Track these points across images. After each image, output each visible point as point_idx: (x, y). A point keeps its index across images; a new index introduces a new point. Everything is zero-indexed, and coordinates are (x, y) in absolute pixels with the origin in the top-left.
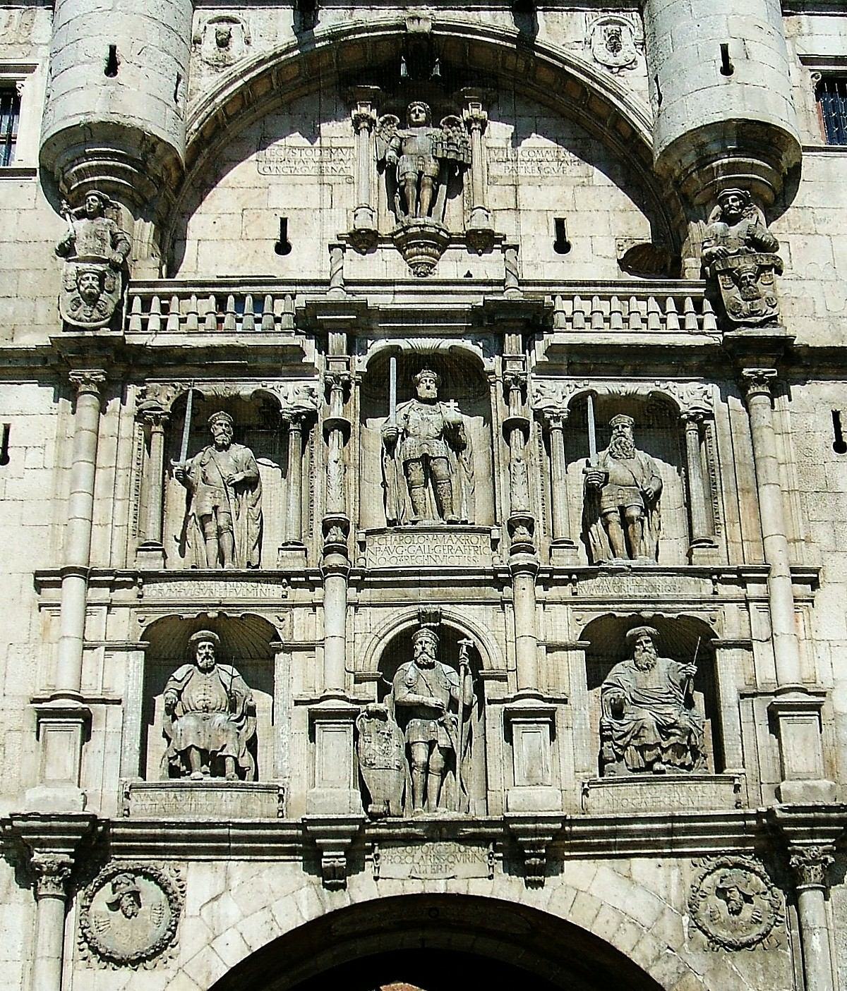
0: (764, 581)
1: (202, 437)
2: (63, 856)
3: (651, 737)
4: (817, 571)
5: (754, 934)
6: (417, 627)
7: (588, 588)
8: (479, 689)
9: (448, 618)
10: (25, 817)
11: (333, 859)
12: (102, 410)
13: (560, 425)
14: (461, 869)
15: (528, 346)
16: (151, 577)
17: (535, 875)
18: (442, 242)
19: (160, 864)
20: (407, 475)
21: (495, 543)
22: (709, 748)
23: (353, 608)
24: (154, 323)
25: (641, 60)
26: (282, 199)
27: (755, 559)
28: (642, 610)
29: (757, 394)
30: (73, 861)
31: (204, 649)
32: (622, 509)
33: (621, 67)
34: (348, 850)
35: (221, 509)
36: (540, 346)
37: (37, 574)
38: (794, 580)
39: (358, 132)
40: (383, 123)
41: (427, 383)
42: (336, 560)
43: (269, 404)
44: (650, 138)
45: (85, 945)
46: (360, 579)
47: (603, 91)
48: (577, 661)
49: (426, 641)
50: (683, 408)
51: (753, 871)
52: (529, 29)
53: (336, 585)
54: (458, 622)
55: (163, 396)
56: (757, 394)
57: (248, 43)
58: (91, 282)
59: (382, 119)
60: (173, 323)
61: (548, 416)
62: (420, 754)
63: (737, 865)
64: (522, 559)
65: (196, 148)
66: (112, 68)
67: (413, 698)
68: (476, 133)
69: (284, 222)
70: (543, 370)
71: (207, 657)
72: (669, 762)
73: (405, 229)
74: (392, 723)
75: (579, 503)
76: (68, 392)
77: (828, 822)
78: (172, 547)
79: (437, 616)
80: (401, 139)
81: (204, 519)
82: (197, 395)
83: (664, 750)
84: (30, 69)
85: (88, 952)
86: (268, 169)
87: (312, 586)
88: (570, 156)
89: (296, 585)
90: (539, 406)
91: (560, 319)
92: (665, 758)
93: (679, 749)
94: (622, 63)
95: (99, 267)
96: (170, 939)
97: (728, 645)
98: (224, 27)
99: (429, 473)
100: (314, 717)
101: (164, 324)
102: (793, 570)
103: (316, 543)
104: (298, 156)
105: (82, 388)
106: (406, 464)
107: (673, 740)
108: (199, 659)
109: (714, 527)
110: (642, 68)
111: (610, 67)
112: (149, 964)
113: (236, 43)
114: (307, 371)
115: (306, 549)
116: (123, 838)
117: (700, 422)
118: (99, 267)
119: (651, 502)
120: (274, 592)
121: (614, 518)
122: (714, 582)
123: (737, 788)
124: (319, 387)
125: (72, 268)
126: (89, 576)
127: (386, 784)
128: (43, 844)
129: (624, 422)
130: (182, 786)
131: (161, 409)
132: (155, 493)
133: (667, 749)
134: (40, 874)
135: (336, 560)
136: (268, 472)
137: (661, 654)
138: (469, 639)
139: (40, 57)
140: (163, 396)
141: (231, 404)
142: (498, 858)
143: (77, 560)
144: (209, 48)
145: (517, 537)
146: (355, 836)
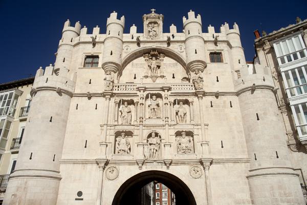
2: (103, 165)
3: (184, 148)
7: (176, 127)
8: (161, 141)
11: (140, 165)
14: (157, 167)
18: (157, 77)
22: (193, 150)
24: (117, 90)
26: (135, 71)
27: (199, 123)
31: (123, 135)
49: (153, 135)
53: (141, 126)
55: (118, 99)
58: (108, 85)
62: (152, 150)
64: (167, 123)
65: (123, 65)
66: (111, 54)
70: (170, 95)
75: (175, 113)
91: (173, 89)
98: (127, 47)
100: (138, 145)
103: (138, 121)
110: (185, 52)
119: (185, 114)
120: (133, 127)
124: (139, 98)
129: (181, 103)
135: (141, 123)
139: (102, 51)
141: (127, 101)
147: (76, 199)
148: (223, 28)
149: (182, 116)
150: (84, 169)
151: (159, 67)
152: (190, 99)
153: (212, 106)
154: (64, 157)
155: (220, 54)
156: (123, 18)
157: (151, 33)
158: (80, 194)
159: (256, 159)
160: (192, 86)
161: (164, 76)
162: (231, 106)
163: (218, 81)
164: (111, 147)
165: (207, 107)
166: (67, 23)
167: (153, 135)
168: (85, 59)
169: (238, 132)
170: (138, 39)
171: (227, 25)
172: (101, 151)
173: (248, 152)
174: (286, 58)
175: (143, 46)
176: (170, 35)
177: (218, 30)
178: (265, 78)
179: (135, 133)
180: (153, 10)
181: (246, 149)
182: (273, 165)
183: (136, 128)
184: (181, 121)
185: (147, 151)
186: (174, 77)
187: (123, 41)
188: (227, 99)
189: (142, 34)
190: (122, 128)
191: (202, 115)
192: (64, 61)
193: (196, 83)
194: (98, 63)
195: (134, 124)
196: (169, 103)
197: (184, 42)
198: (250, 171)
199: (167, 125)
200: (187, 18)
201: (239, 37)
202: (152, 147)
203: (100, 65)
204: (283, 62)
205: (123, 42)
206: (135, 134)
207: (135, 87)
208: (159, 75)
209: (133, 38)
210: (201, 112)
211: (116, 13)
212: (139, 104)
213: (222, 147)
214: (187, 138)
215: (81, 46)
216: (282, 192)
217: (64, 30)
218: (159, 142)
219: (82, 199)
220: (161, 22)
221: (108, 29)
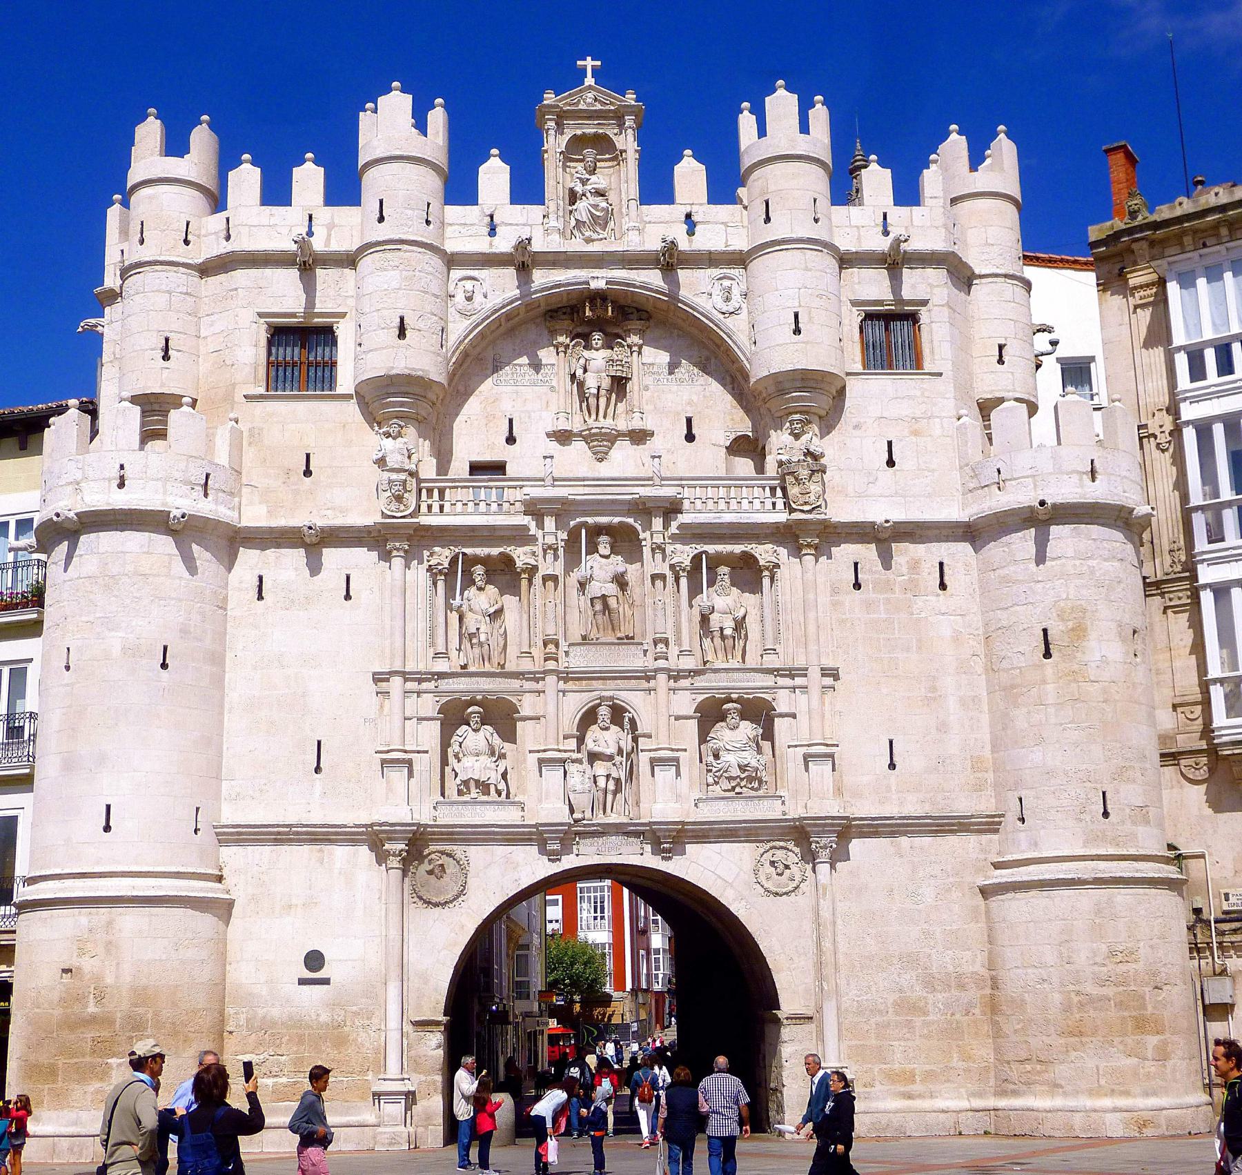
0: (805, 675)
1: (469, 582)
3: (735, 772)
4: (837, 669)
5: (790, 888)
6: (600, 705)
7: (700, 682)
8: (635, 740)
9: (617, 699)
10: (381, 825)
12: (407, 566)
13: (685, 574)
15: (666, 526)
16: (441, 676)
17: (667, 854)
18: (612, 438)
19: (455, 848)
20: (592, 605)
21: (645, 651)
23: (561, 694)
24: (436, 508)
25: (744, 306)
26: (508, 407)
27: (800, 662)
28: (731, 693)
29: (806, 554)
30: (407, 848)
31: (475, 719)
32: (722, 629)
33: (731, 313)
34: (562, 840)
35: (481, 631)
36: (674, 525)
37: (374, 674)
38: (823, 675)
39: (558, 354)
40: (573, 346)
41: (604, 547)
42: (551, 665)
43: (508, 561)
44: (748, 367)
45: (414, 895)
46: (566, 676)
47: (718, 331)
48: (693, 725)
49: (604, 711)
50: (762, 563)
51: (791, 851)
52: (674, 283)
53: (551, 679)
54: (623, 702)
55: (442, 555)
56: (806, 554)
57: (486, 297)
59: (573, 342)
60: (447, 508)
61: (678, 569)
62: (602, 782)
63: (782, 848)
66: (402, 333)
67: (597, 749)
68: (635, 354)
69: (511, 421)
70: (674, 538)
71: (477, 722)
72: (745, 786)
73: (590, 429)
74: (586, 765)
76: (386, 556)
77: (833, 825)
78: (453, 654)
79: (612, 698)
80: (586, 360)
81: (471, 636)
82: (464, 554)
83: (742, 779)
84: (343, 315)
85: (416, 899)
86: (498, 381)
87: (537, 680)
88: (696, 370)
89: (528, 679)
90: (672, 562)
92: (743, 784)
93: (750, 779)
94: (732, 310)
95: (403, 476)
96: (462, 891)
97: (782, 715)
98: (469, 285)
99: (606, 606)
101: (442, 507)
102: (822, 669)
103: (538, 652)
104: (518, 371)
105: (395, 553)
106: (592, 599)
107: (746, 774)
108: (472, 724)
109: (777, 640)
111: (724, 313)
112: (451, 905)
113: (478, 298)
114: (532, 540)
115: (533, 657)
116: (434, 833)
117: (771, 571)
118: (403, 476)
120: (515, 684)
121: (717, 634)
122: (776, 676)
123: (783, 803)
124: (539, 550)
125: (386, 475)
126: (406, 676)
127: (582, 801)
128: (390, 839)
129: (723, 570)
130: (466, 802)
131: (442, 565)
132: (441, 619)
133: (744, 778)
134: (389, 855)
135: (551, 665)
136: (509, 601)
137: (742, 718)
138: (630, 713)
140: (442, 555)
141: (484, 561)
142: (647, 843)
143: (398, 667)
144: (460, 298)
145: (658, 650)
146: (566, 833)
147: (302, 982)
148: (931, 179)
149: (728, 632)
150: (321, 861)
151: (619, 385)
152: (764, 552)
153: (857, 586)
154: (231, 815)
155: (913, 318)
156: (437, 117)
157: (581, 205)
158: (314, 960)
159: (1023, 820)
160: (773, 489)
161: (639, 437)
162: (943, 586)
163: (891, 463)
164: (427, 765)
165: (835, 591)
166: (150, 132)
167: (604, 711)
168: (270, 343)
169: (962, 702)
170: (523, 245)
171: (956, 144)
172: (390, 789)
173: (996, 785)
174: (1210, 356)
175: (542, 278)
176: (675, 212)
177: (907, 193)
178: (1096, 463)
179: (527, 706)
180: (589, 63)
181: (990, 776)
182: (1086, 843)
183: (528, 685)
184: (720, 655)
185: (579, 787)
186: (690, 437)
187: (451, 246)
188: (928, 554)
189: (535, 211)
190: (475, 687)
191: (812, 629)
192: (166, 357)
193: (790, 479)
194: (333, 365)
195: (520, 669)
196: (669, 574)
197: (740, 260)
198: (997, 866)
199: (662, 677)
200: (762, 132)
201: (1010, 214)
202: (601, 768)
203: (346, 380)
204: (1197, 372)
205: (453, 261)
206: (525, 711)
207: (518, 495)
208: (622, 425)
209: (492, 231)
210: (812, 615)
211: (408, 99)
212: (538, 580)
213: (892, 766)
214: (747, 729)
215: (242, 277)
216: (1104, 948)
217: (133, 177)
218: (627, 744)
219: (326, 981)
220: (627, 142)
221: (374, 183)
